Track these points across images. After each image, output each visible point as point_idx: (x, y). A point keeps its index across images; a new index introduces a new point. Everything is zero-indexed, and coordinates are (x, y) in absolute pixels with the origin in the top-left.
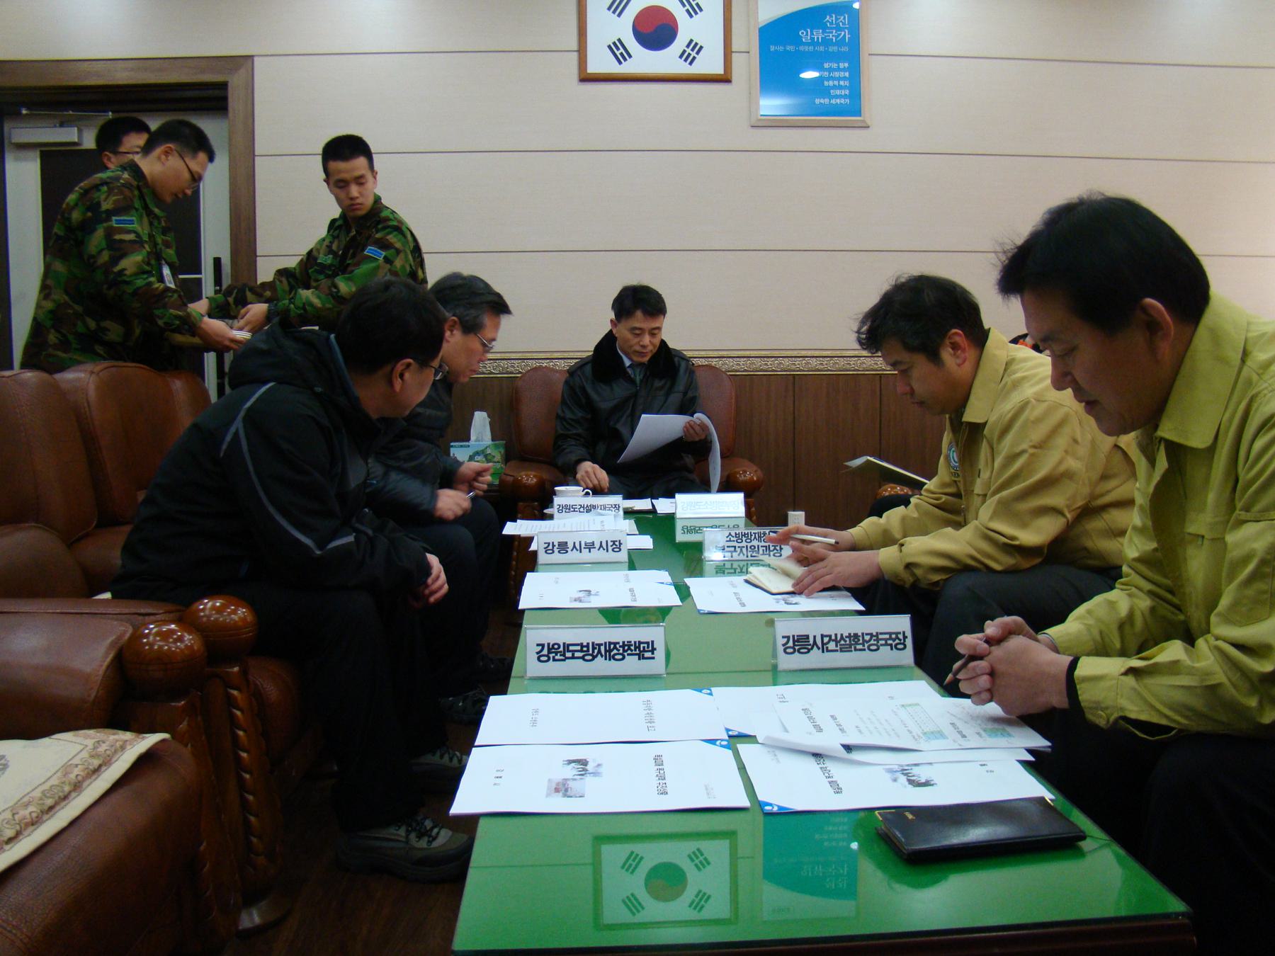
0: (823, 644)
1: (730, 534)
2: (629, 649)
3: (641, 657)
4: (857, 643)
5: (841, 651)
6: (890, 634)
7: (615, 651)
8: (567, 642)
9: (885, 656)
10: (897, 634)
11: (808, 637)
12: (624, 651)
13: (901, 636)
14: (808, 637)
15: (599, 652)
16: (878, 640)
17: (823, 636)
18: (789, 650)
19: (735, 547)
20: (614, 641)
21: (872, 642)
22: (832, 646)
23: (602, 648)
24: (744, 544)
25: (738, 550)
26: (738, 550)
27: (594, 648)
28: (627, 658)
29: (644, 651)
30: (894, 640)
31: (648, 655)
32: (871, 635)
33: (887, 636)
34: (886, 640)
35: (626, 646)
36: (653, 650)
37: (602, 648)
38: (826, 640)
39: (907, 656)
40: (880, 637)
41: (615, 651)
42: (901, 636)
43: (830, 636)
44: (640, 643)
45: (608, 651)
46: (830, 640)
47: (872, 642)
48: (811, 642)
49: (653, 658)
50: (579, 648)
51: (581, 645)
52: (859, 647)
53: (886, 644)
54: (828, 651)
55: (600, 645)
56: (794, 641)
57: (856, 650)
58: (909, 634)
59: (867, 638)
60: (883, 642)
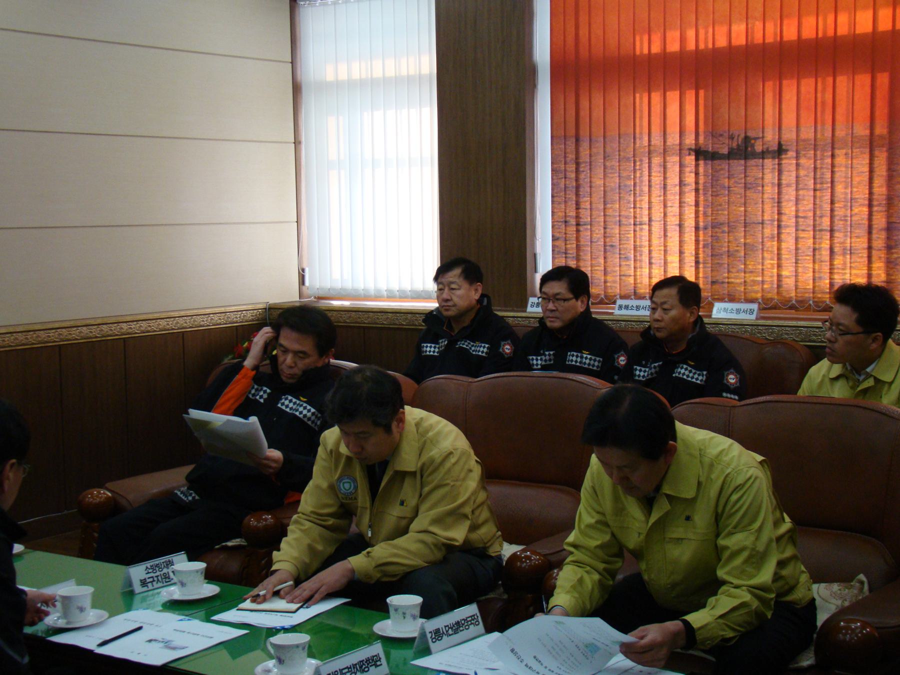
0: (447, 631)
1: (147, 568)
2: (370, 662)
3: (377, 666)
4: (460, 627)
5: (455, 634)
6: (471, 617)
7: (364, 666)
8: (341, 668)
9: (474, 630)
10: (474, 615)
11: (439, 629)
12: (368, 664)
13: (476, 617)
14: (439, 629)
15: (357, 669)
16: (467, 622)
17: (445, 627)
18: (434, 640)
19: (152, 577)
20: (361, 660)
21: (466, 624)
22: (450, 632)
23: (358, 666)
24: (158, 573)
25: (156, 579)
26: (156, 579)
27: (354, 668)
28: (371, 668)
29: (377, 661)
30: (473, 620)
31: (378, 663)
32: (463, 619)
33: (470, 619)
34: (470, 621)
35: (368, 660)
36: (380, 659)
37: (358, 666)
38: (447, 628)
39: (481, 628)
40: (468, 619)
41: (364, 666)
42: (476, 617)
43: (448, 626)
44: (373, 657)
45: (361, 667)
46: (449, 628)
47: (466, 624)
48: (442, 632)
49: (381, 665)
50: (346, 670)
51: (347, 668)
52: (461, 629)
53: (472, 624)
54: (450, 635)
55: (356, 665)
56: (435, 634)
57: (461, 631)
58: (478, 614)
59: (463, 622)
60: (470, 623)
